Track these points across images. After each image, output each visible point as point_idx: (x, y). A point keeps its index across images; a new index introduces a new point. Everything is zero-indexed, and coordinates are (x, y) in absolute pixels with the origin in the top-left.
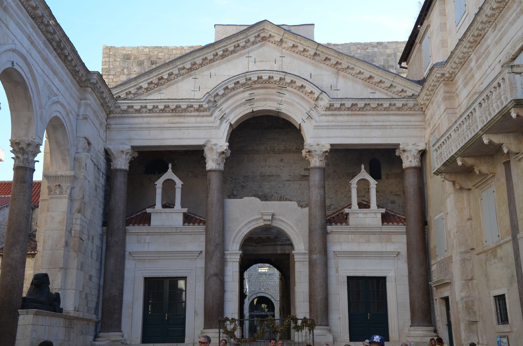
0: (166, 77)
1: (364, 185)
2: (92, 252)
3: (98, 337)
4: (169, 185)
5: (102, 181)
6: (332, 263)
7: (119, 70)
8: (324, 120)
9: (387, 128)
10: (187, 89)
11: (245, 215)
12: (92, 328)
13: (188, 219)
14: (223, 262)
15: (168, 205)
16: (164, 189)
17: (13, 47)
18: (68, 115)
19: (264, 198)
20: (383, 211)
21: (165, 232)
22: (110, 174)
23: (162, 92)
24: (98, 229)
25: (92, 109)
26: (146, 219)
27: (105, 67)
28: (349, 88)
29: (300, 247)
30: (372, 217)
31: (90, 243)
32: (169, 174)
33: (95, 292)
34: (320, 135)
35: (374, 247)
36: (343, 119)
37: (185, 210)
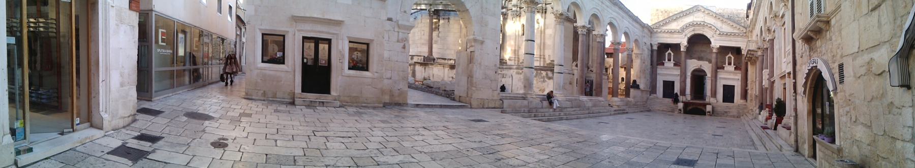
1: (730, 58)
4: (669, 54)
6: (718, 81)
8: (718, 38)
10: (674, 26)
11: (693, 64)
13: (675, 65)
14: (685, 78)
15: (669, 60)
19: (700, 59)
21: (668, 68)
22: (652, 51)
24: (649, 66)
26: (663, 64)
28: (726, 28)
29: (709, 75)
30: (732, 68)
32: (670, 51)
34: (716, 43)
35: (732, 76)
36: (723, 38)
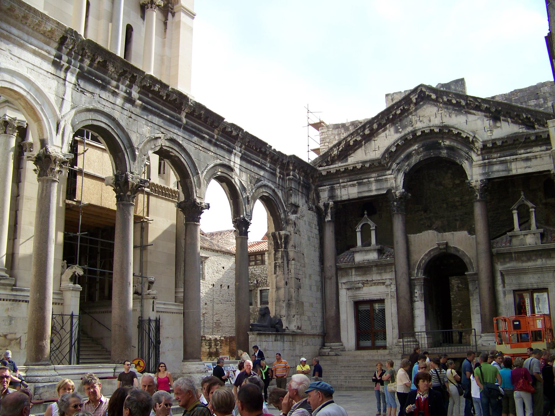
0: (351, 143)
2: (310, 286)
3: (325, 346)
5: (316, 232)
7: (332, 137)
9: (536, 158)
12: (319, 341)
16: (362, 232)
17: (218, 162)
18: (274, 191)
20: (541, 230)
23: (352, 155)
25: (295, 181)
27: (322, 137)
31: (307, 280)
33: (319, 315)
37: (379, 247)
